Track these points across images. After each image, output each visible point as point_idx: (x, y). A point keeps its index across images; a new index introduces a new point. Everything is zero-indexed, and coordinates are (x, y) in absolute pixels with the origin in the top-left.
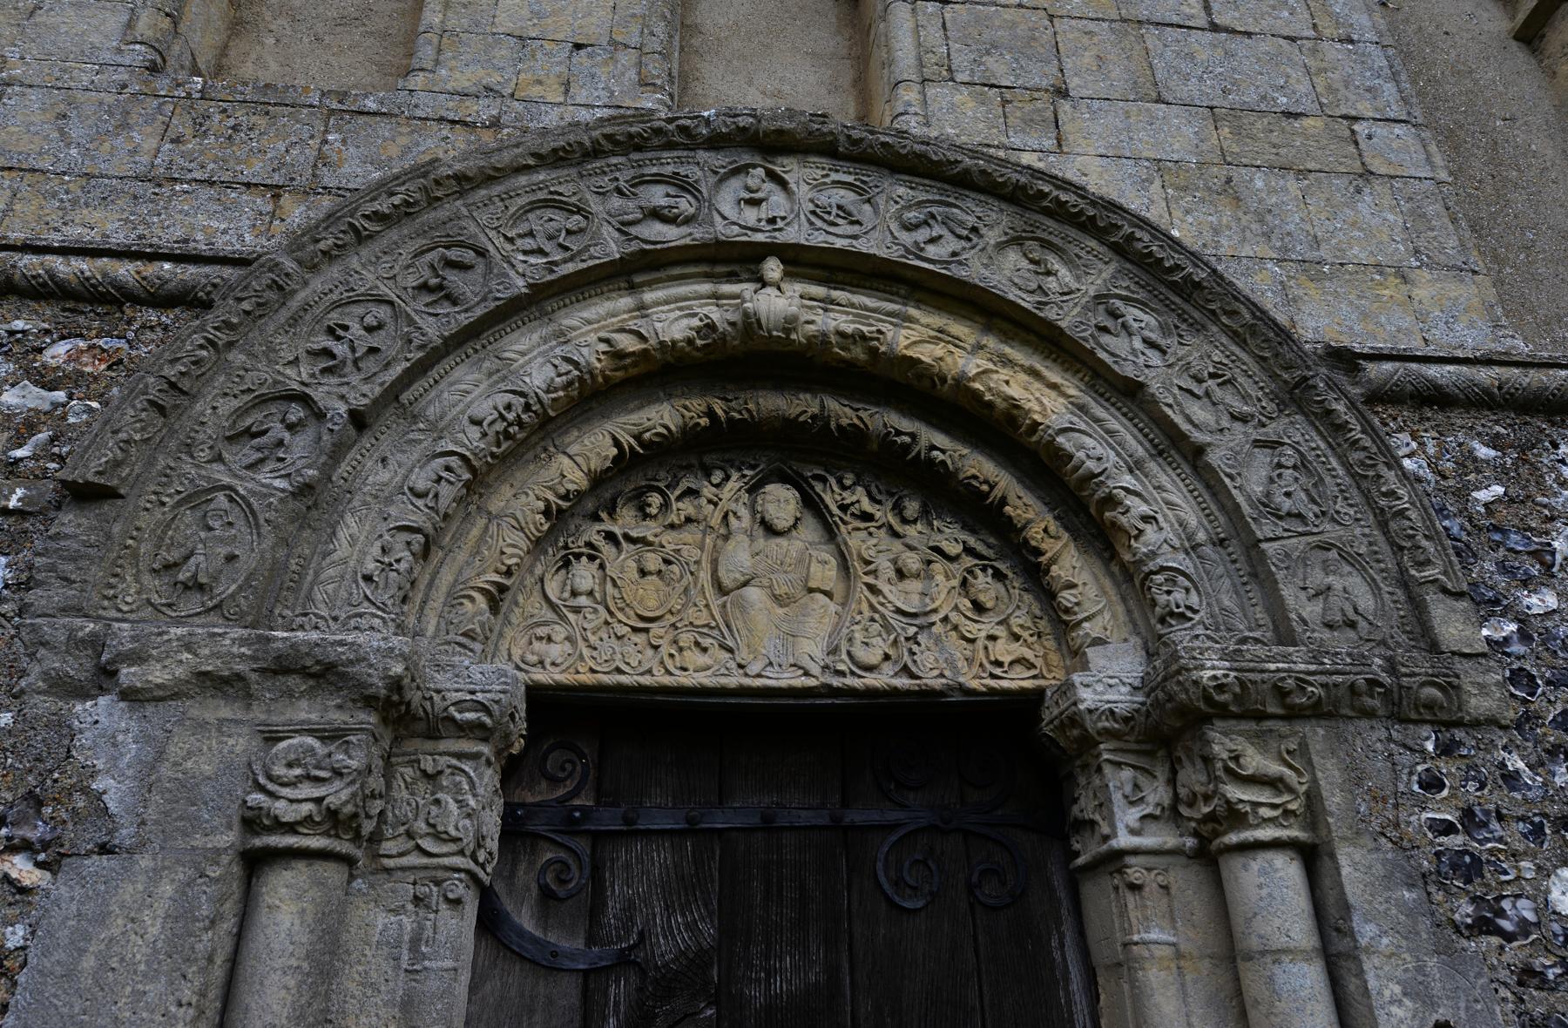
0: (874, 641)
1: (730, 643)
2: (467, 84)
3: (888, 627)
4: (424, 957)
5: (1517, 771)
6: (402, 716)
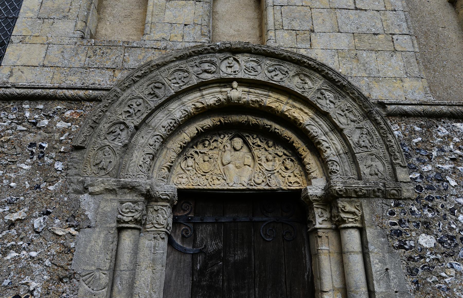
0: (260, 177)
1: (225, 178)
2: (158, 37)
3: (264, 174)
4: (157, 250)
5: (414, 211)
6: (149, 197)
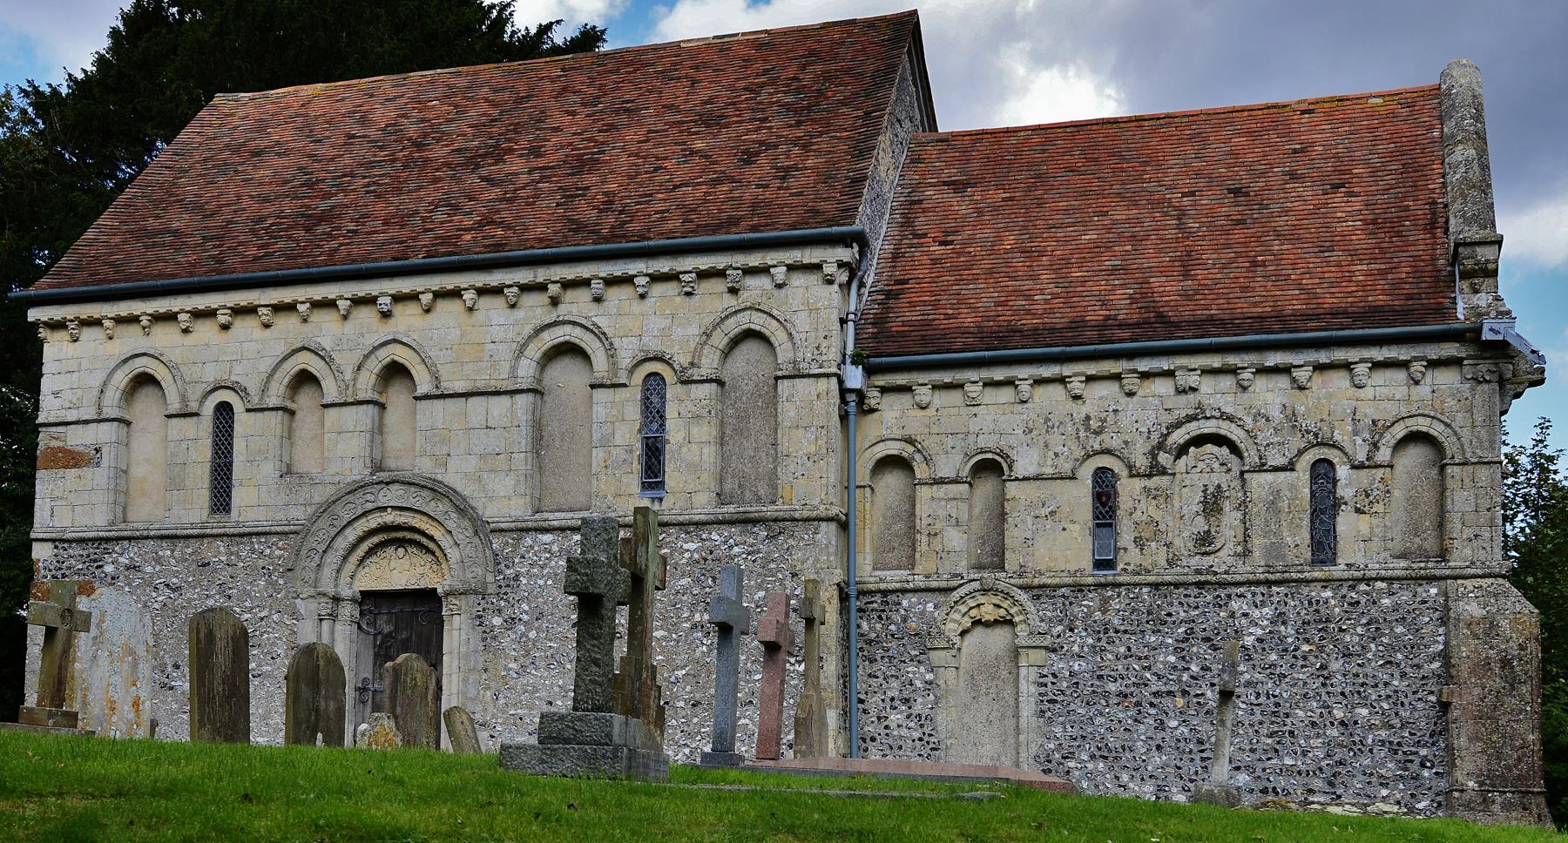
6: (337, 600)
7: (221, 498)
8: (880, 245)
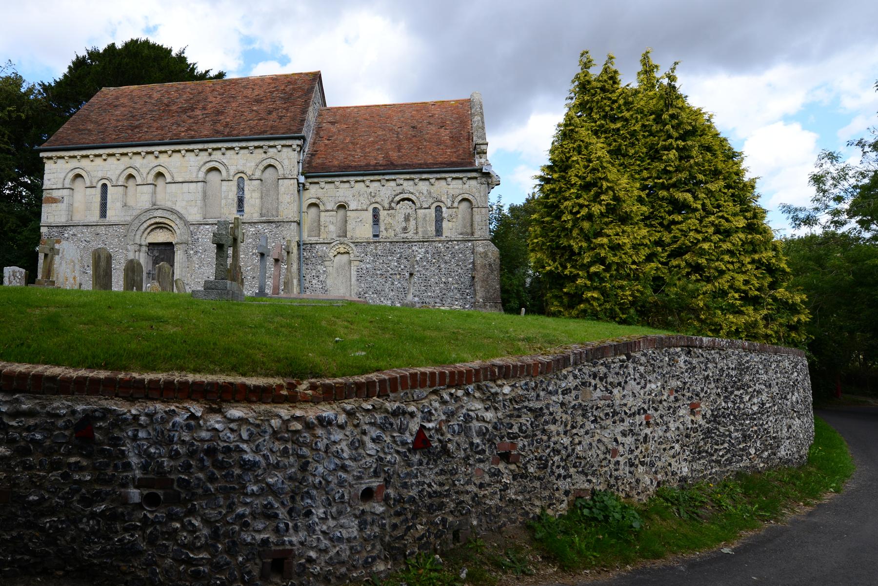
6: (140, 245)
7: (103, 213)
8: (309, 140)
